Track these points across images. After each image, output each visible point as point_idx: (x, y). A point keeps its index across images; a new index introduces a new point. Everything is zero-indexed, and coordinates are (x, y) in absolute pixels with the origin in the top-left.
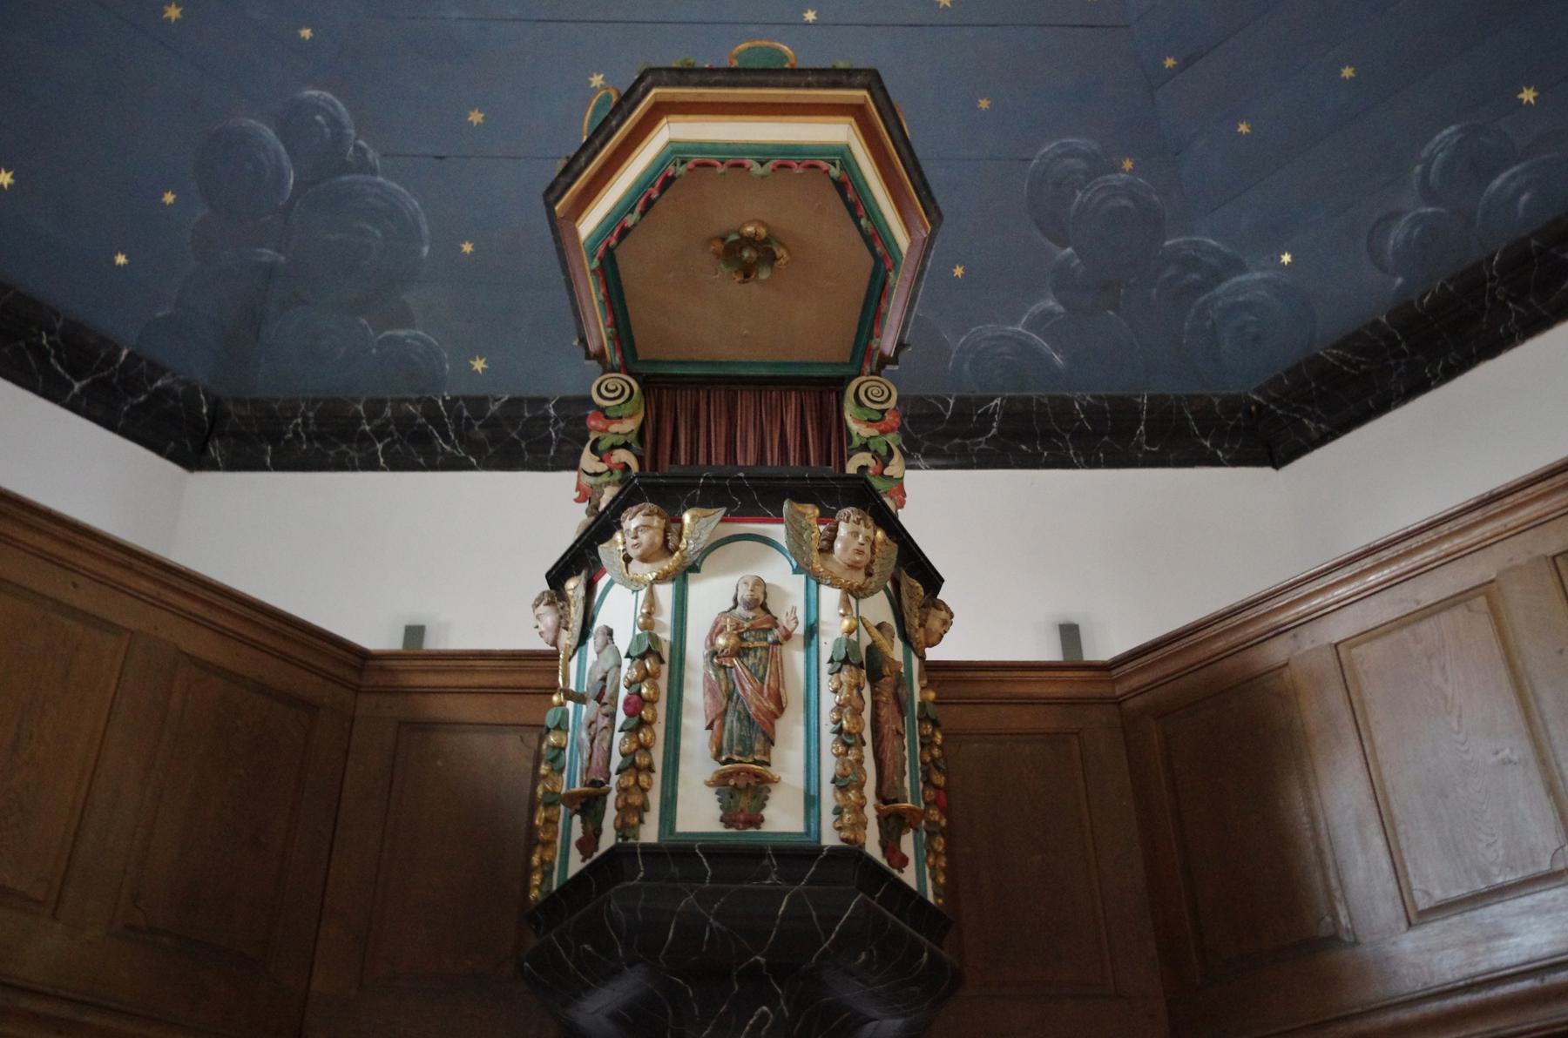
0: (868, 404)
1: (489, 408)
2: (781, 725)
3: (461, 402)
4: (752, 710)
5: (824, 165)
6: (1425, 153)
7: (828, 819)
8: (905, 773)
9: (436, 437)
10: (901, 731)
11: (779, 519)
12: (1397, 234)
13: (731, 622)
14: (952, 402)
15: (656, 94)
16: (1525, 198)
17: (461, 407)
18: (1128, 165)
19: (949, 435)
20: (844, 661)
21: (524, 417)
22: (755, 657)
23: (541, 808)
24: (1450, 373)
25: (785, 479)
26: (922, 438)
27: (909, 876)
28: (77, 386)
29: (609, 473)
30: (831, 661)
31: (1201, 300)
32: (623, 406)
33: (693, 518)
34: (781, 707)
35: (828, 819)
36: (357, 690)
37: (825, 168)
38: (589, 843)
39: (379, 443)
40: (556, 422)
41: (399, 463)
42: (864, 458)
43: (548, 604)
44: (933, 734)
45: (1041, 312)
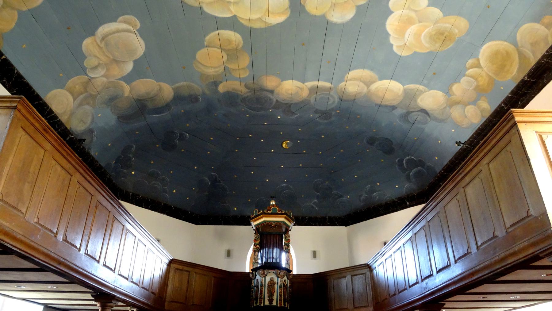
7: (278, 304)
11: (275, 270)
12: (362, 198)
14: (301, 217)
16: (377, 197)
20: (281, 287)
34: (274, 291)
35: (278, 304)
38: (256, 303)
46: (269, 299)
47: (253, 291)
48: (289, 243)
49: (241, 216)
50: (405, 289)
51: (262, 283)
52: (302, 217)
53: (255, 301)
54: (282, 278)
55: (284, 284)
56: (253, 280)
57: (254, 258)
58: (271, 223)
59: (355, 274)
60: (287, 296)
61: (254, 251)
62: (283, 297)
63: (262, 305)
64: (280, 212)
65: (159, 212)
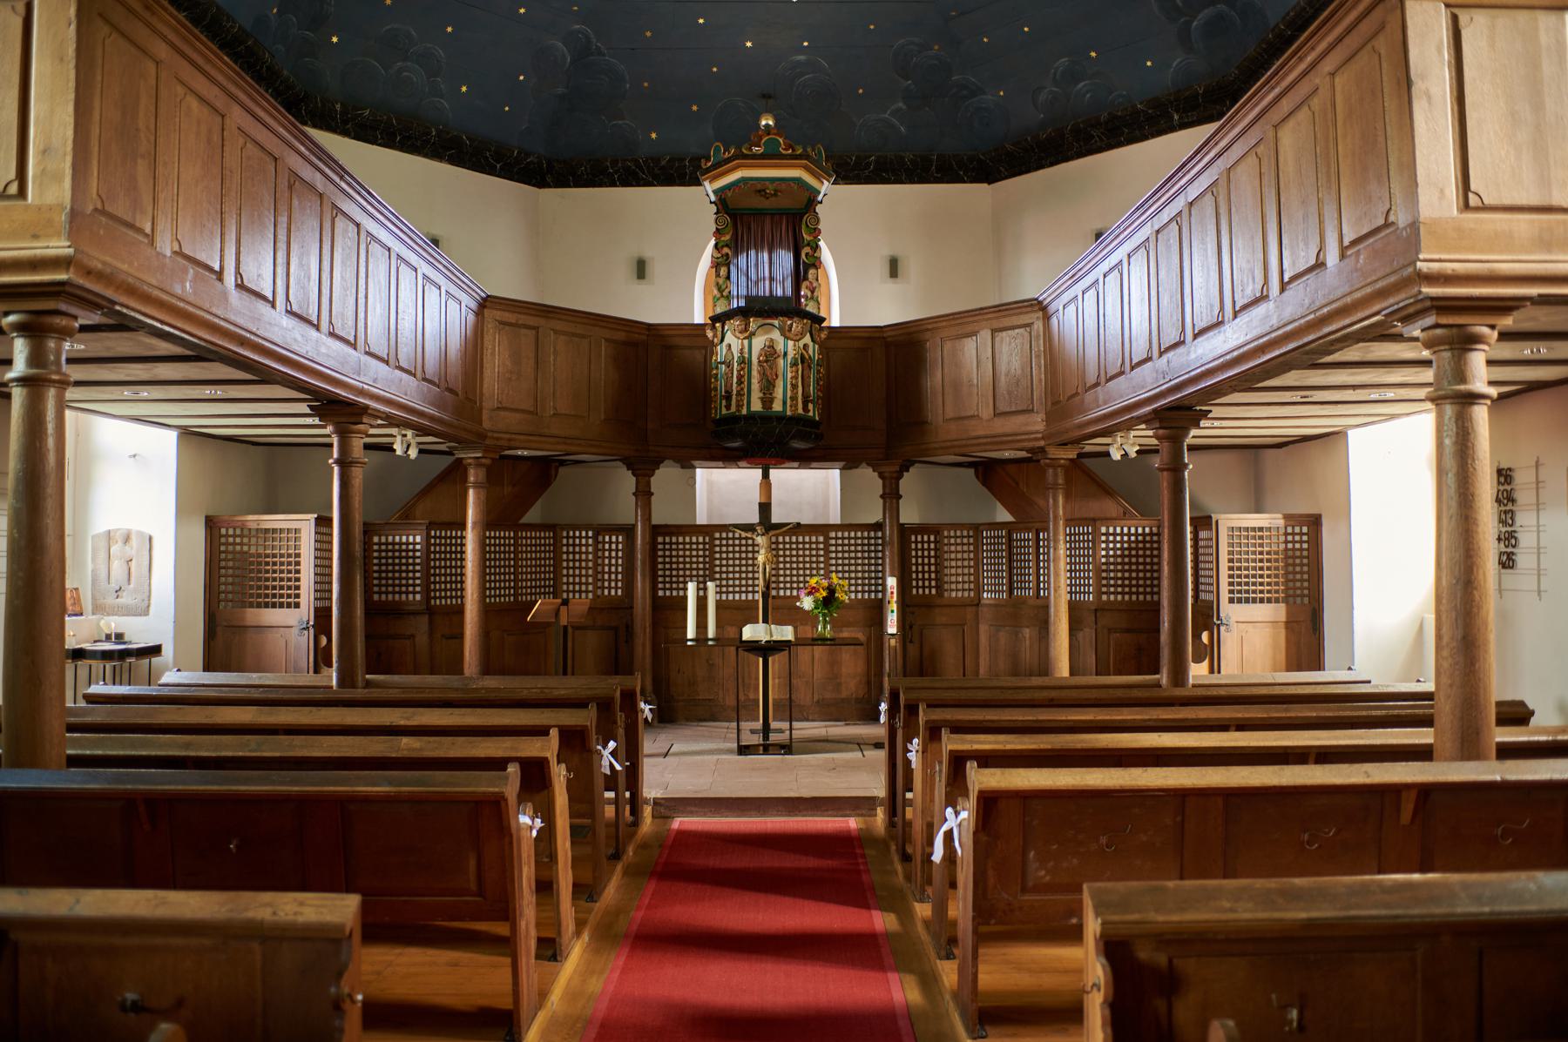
5: (792, 185)
6: (1055, 66)
12: (1042, 97)
14: (854, 158)
16: (1088, 95)
18: (936, 47)
20: (794, 364)
24: (1052, 164)
27: (811, 414)
28: (498, 166)
31: (967, 103)
38: (728, 407)
41: (626, 183)
46: (761, 395)
50: (1122, 373)
53: (724, 402)
54: (798, 341)
55: (802, 354)
56: (717, 345)
57: (718, 284)
59: (1001, 326)
60: (811, 388)
61: (716, 265)
62: (800, 389)
65: (426, 156)
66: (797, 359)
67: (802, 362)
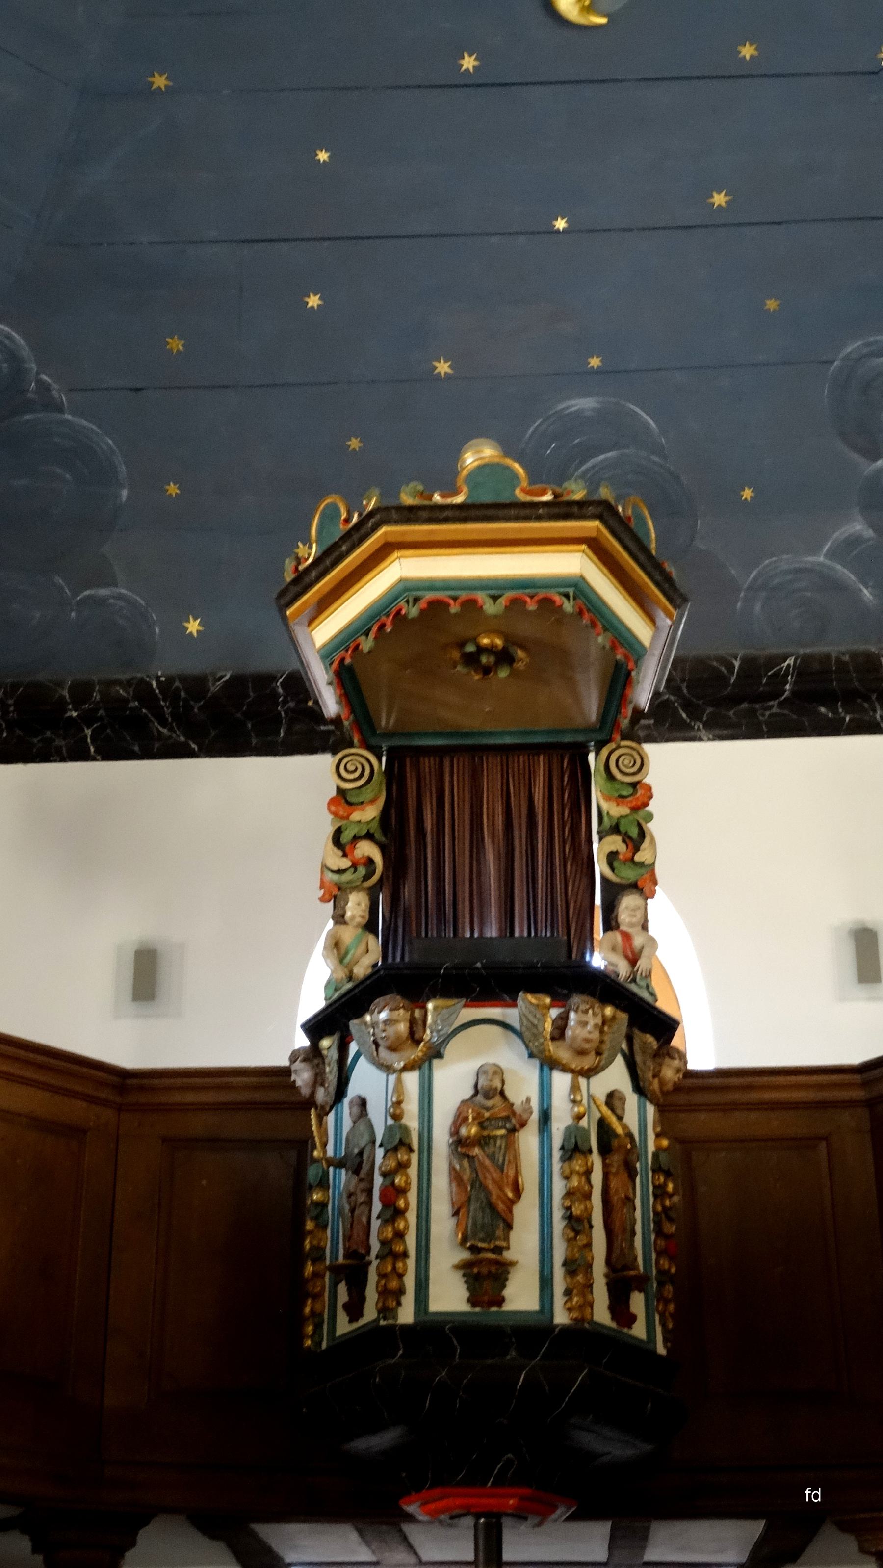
0: (618, 776)
1: (209, 690)
2: (518, 1209)
3: (177, 684)
4: (494, 1198)
5: (558, 599)
7: (559, 1300)
8: (634, 1234)
9: (151, 721)
10: (631, 1195)
13: (472, 1112)
14: (737, 664)
15: (385, 533)
17: (177, 689)
19: (734, 700)
21: (249, 696)
22: (495, 1145)
23: (309, 1263)
25: (520, 968)
26: (703, 703)
27: (639, 1330)
29: (352, 870)
30: (562, 1148)
32: (364, 789)
33: (435, 1008)
34: (518, 1192)
35: (559, 1300)
36: (120, 1108)
37: (558, 604)
38: (355, 1309)
39: (88, 728)
40: (285, 702)
42: (614, 842)
43: (305, 1060)
44: (665, 1185)
45: (846, 538)
46: (465, 1255)
47: (322, 1206)
48: (641, 813)
49: (238, 682)
51: (397, 1117)
52: (747, 662)
54: (589, 1073)
55: (603, 1124)
58: (471, 605)
63: (406, 1315)
64: (548, 497)
66: (586, 1133)
67: (605, 1150)
